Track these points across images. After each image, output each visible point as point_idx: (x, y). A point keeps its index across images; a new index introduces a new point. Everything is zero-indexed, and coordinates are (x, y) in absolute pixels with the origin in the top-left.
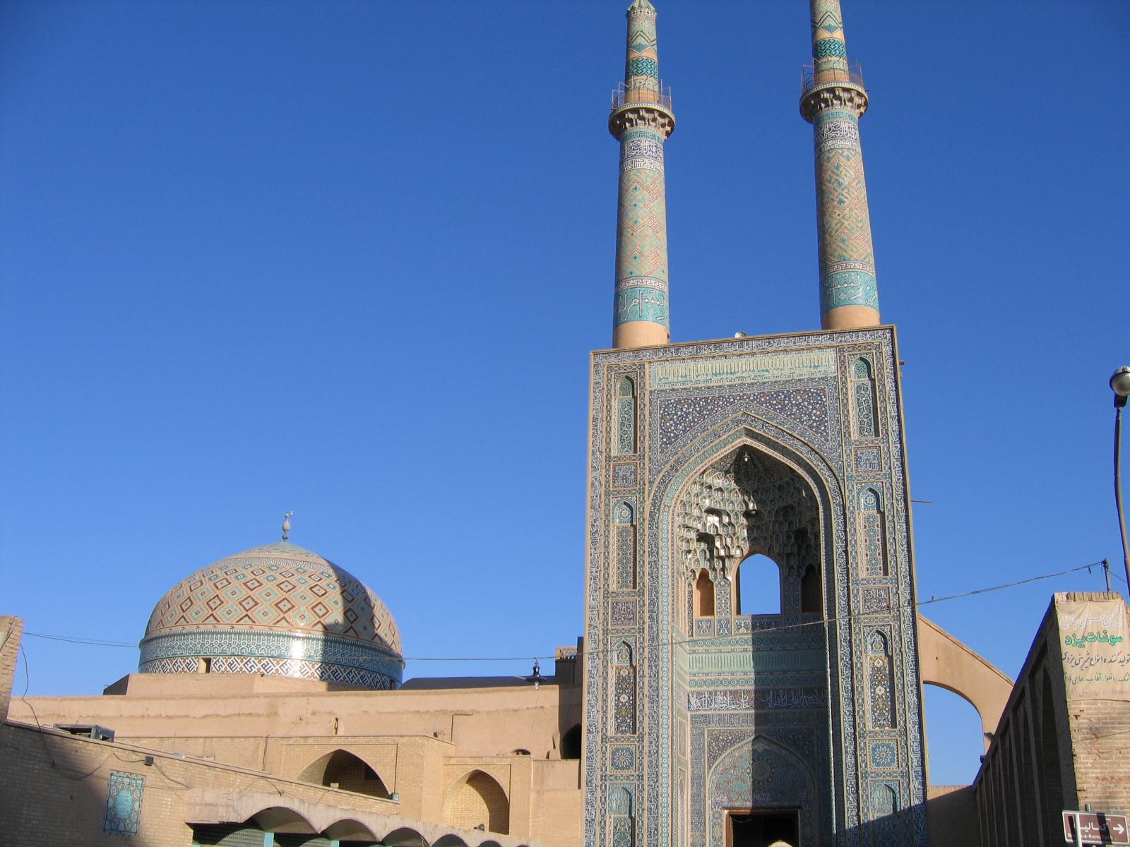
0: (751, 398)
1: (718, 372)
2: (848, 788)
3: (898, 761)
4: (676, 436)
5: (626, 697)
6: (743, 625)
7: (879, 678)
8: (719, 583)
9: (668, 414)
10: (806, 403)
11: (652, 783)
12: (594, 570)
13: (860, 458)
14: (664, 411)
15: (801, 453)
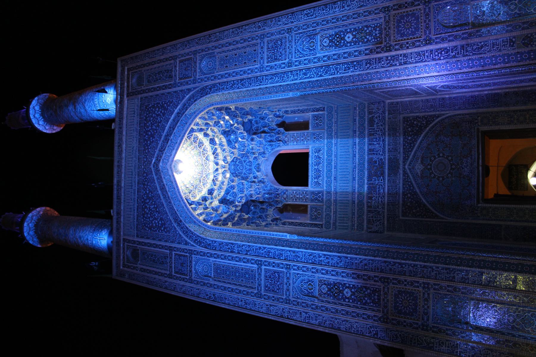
0: (145, 160)
1: (130, 184)
2: (442, 58)
3: (414, 10)
4: (161, 219)
5: (346, 290)
6: (316, 180)
7: (338, 39)
8: (285, 199)
9: (149, 224)
10: (151, 119)
11: (433, 274)
12: (240, 303)
13: (184, 75)
14: (147, 227)
15: (178, 121)
